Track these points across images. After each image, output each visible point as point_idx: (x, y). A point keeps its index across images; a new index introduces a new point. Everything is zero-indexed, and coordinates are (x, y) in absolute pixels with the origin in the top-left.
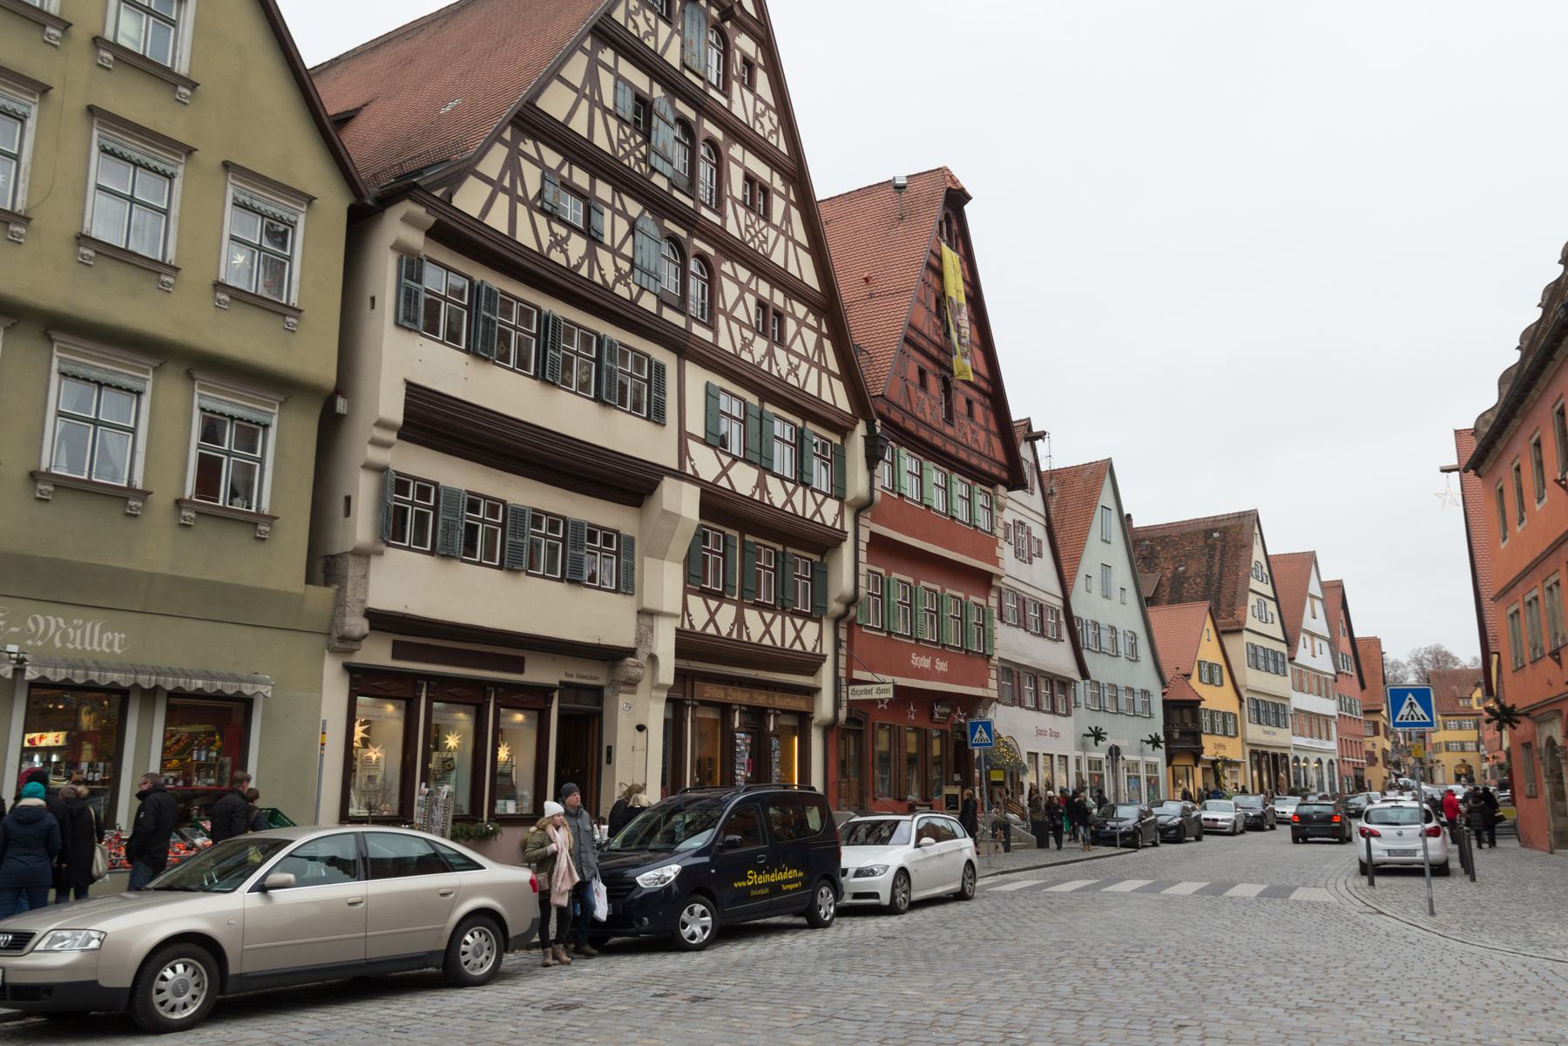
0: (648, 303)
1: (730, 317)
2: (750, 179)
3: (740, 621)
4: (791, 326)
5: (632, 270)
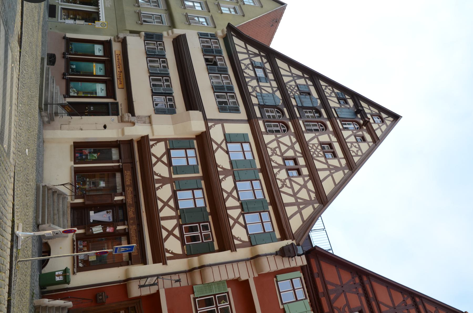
0: (255, 101)
3: (164, 181)
4: (300, 180)
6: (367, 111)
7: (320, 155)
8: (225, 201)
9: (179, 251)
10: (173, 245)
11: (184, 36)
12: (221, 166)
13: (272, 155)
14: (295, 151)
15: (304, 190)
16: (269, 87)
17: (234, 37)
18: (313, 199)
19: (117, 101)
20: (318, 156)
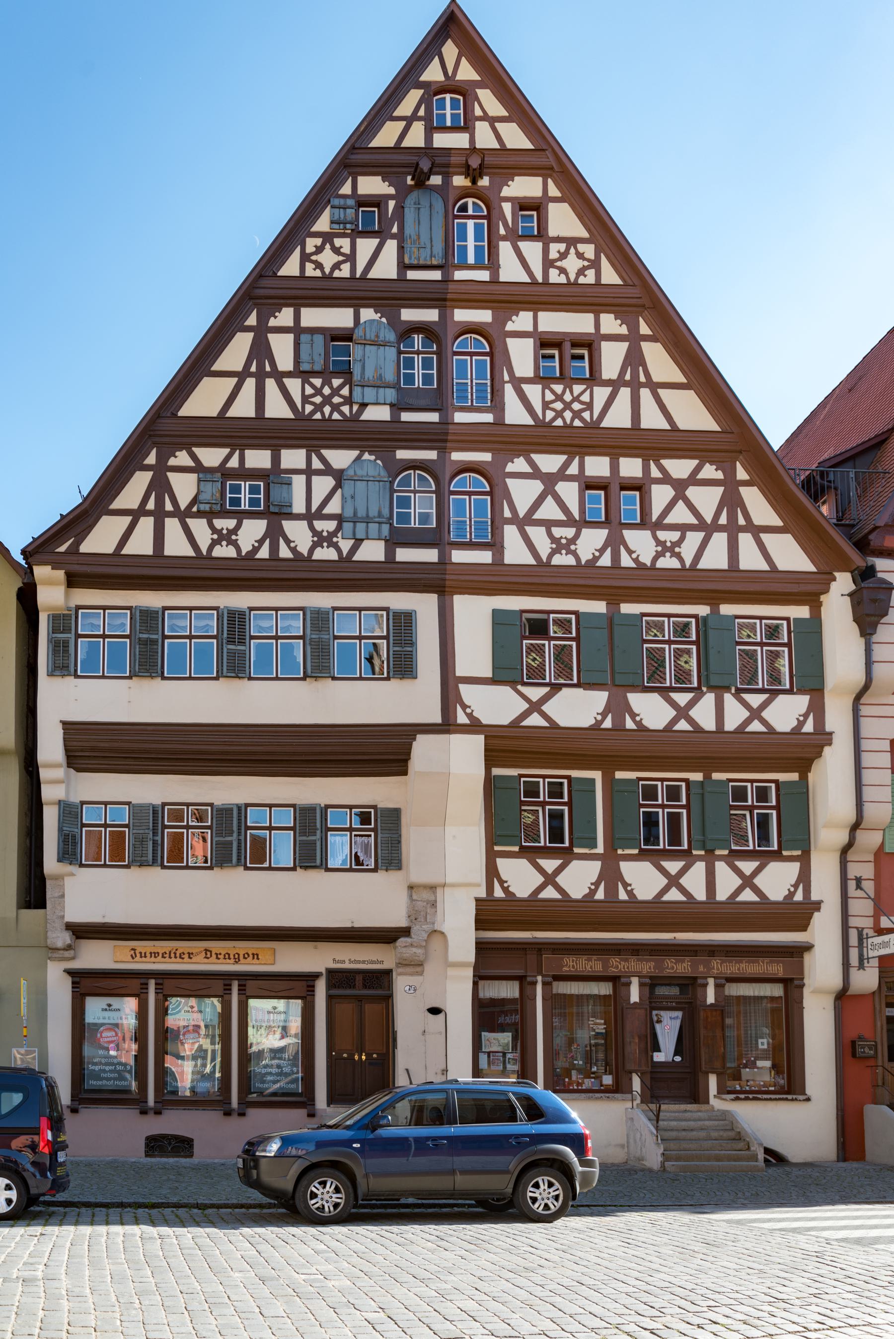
0: (372, 551)
1: (523, 523)
2: (546, 343)
3: (611, 876)
4: (661, 495)
5: (339, 528)
6: (416, 138)
7: (586, 398)
8: (698, 729)
9: (794, 868)
10: (777, 880)
11: (69, 727)
12: (599, 718)
13: (575, 554)
14: (561, 475)
15: (692, 492)
16: (311, 483)
17: (84, 548)
18: (719, 475)
19: (324, 971)
20: (589, 406)
